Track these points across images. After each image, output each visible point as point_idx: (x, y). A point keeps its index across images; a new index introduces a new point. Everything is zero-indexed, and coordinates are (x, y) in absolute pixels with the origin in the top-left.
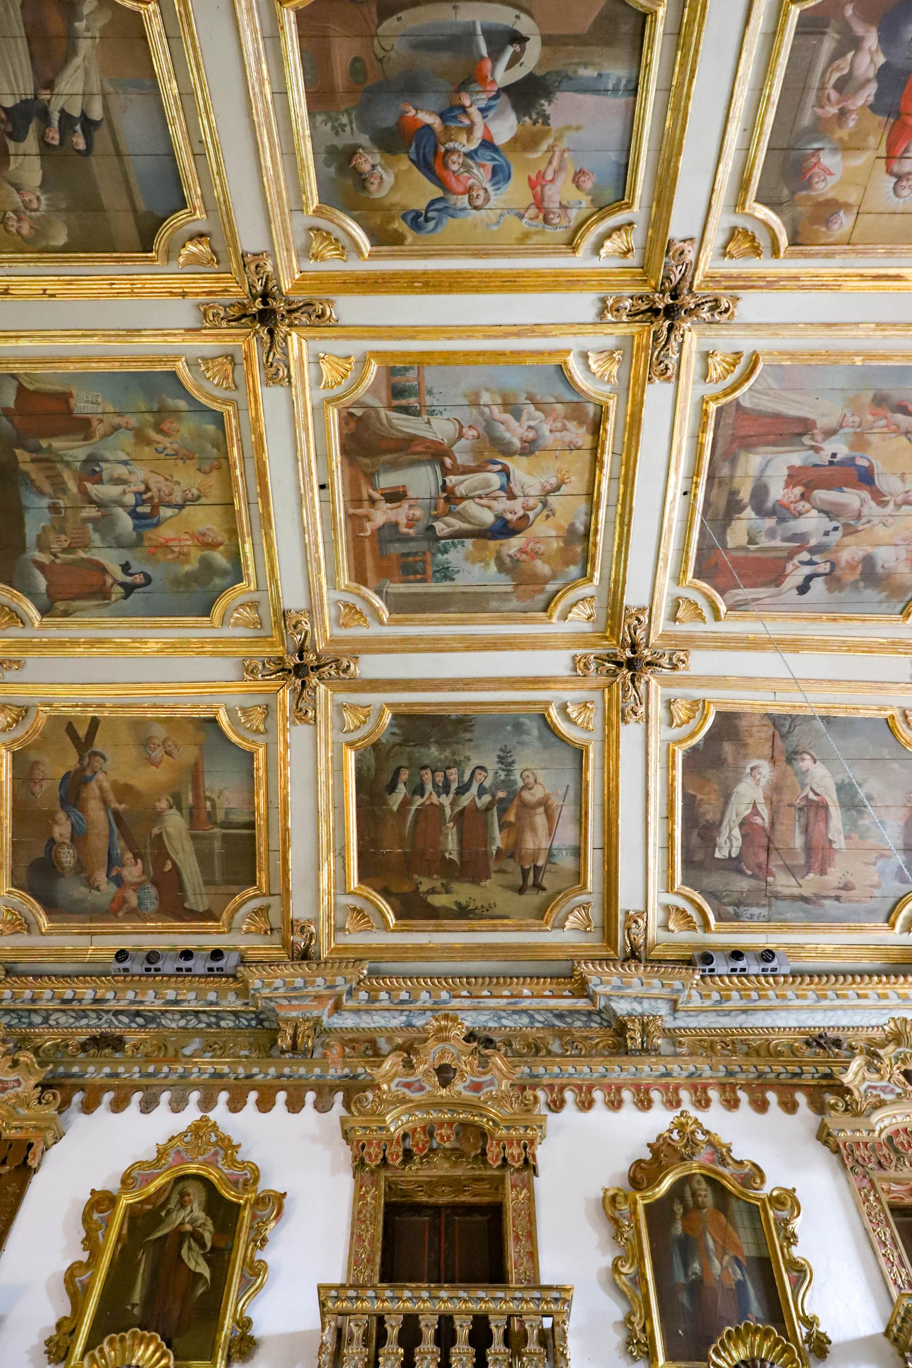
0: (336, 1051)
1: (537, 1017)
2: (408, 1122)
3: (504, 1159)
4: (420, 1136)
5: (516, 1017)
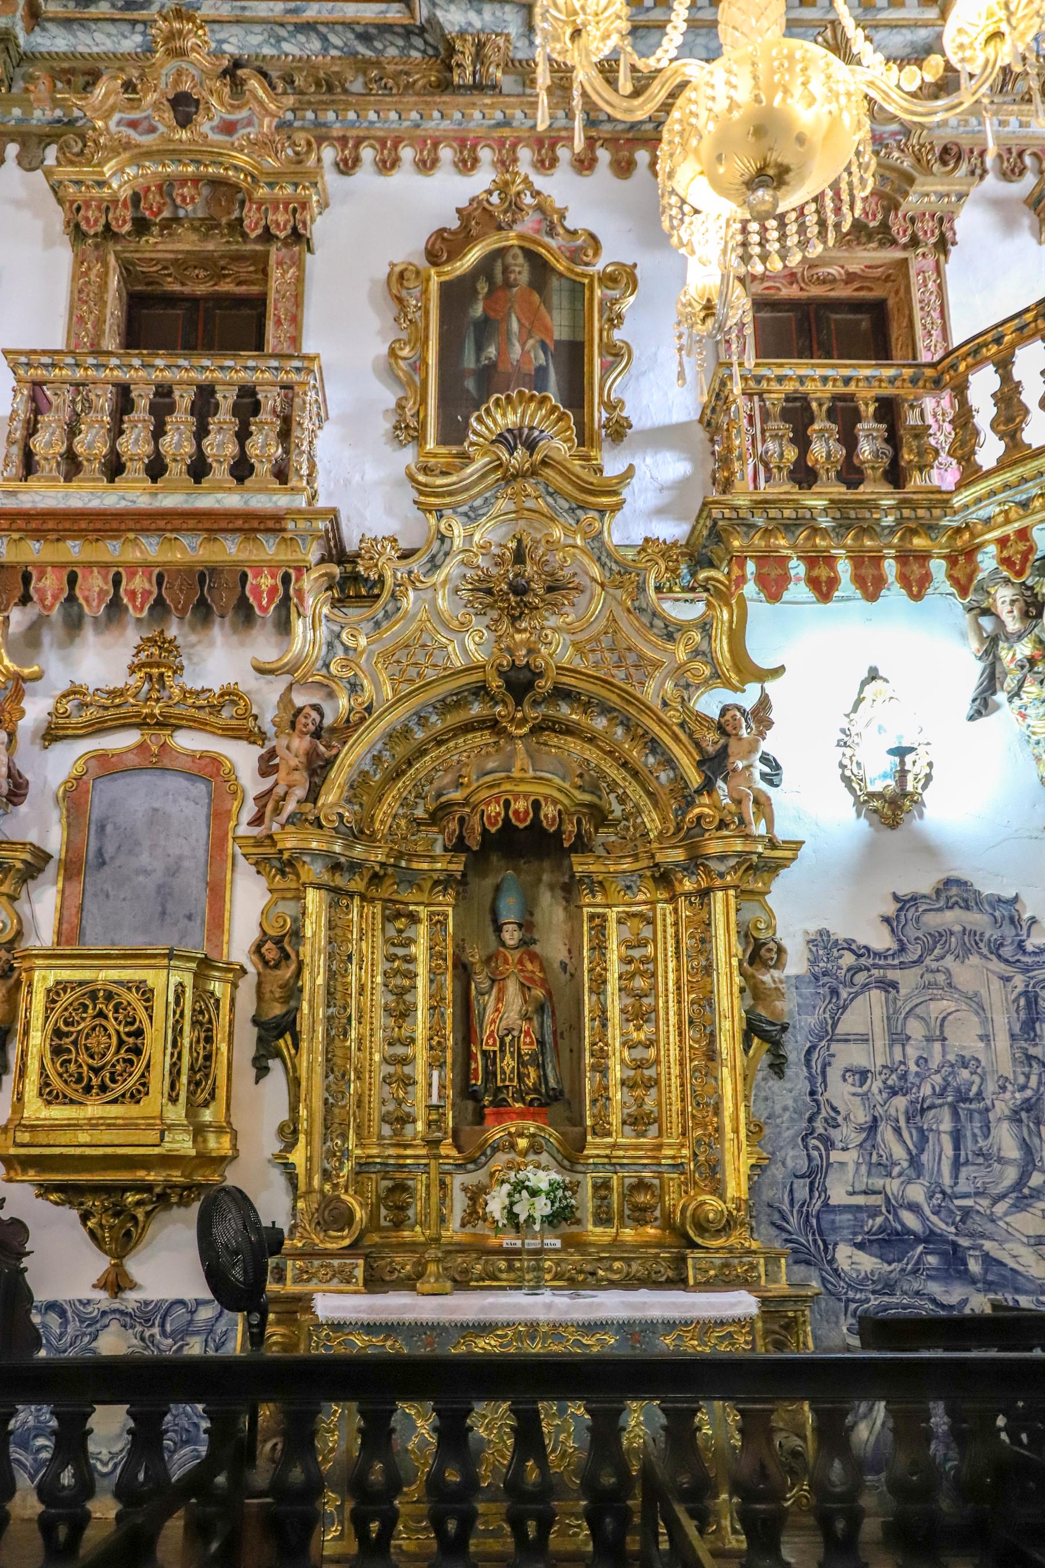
0: (42, 87)
1: (334, 39)
2: (135, 177)
3: (267, 228)
4: (154, 198)
5: (302, 38)
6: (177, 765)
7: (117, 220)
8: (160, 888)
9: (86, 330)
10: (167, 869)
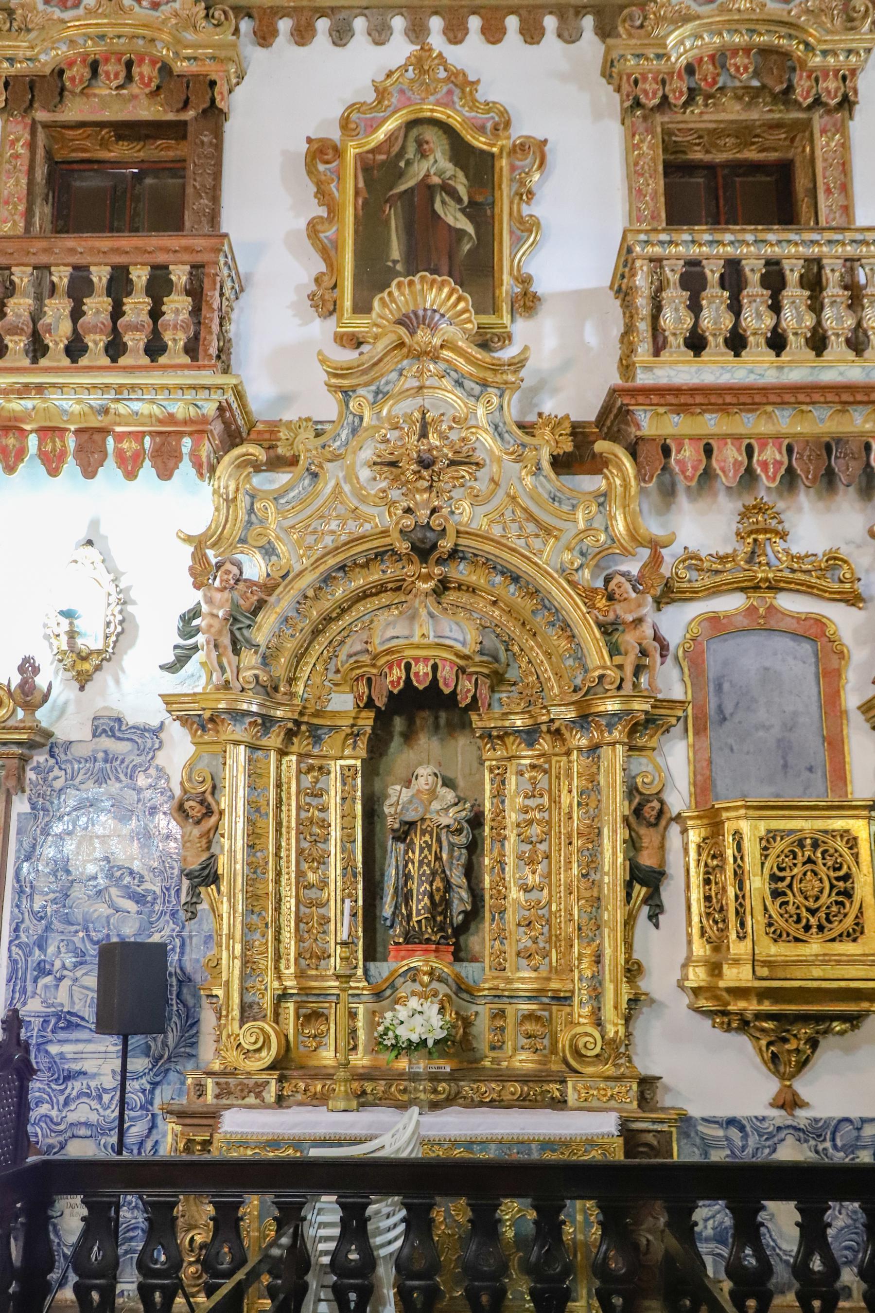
2: (691, 49)
6: (782, 626)
7: (674, 91)
8: (779, 741)
9: (646, 203)
10: (784, 725)
